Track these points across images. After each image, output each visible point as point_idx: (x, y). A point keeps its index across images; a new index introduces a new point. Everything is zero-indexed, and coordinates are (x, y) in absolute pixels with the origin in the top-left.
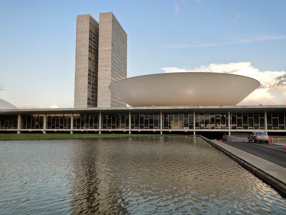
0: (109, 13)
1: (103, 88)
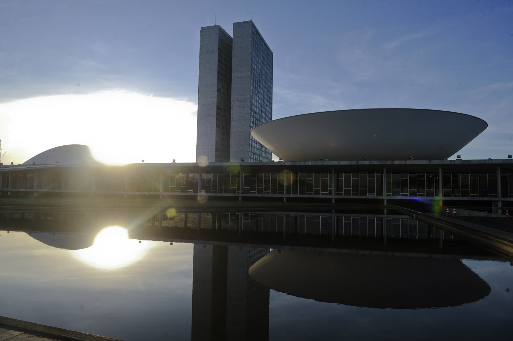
0: (247, 22)
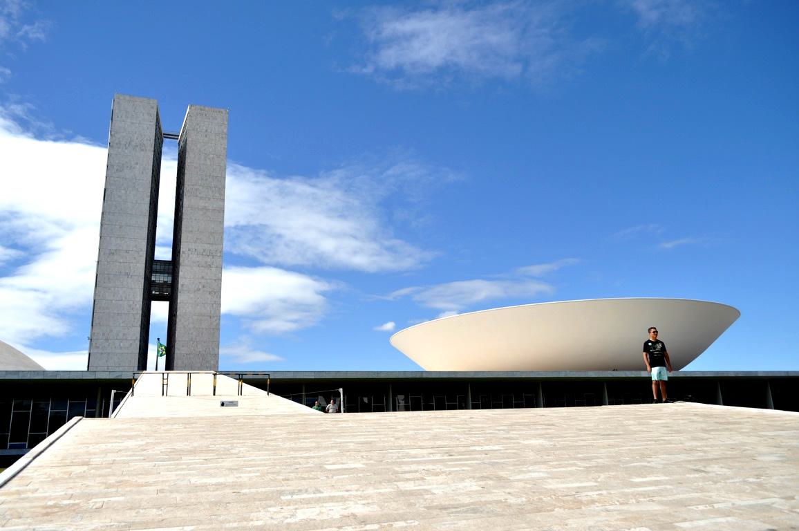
1: (195, 317)
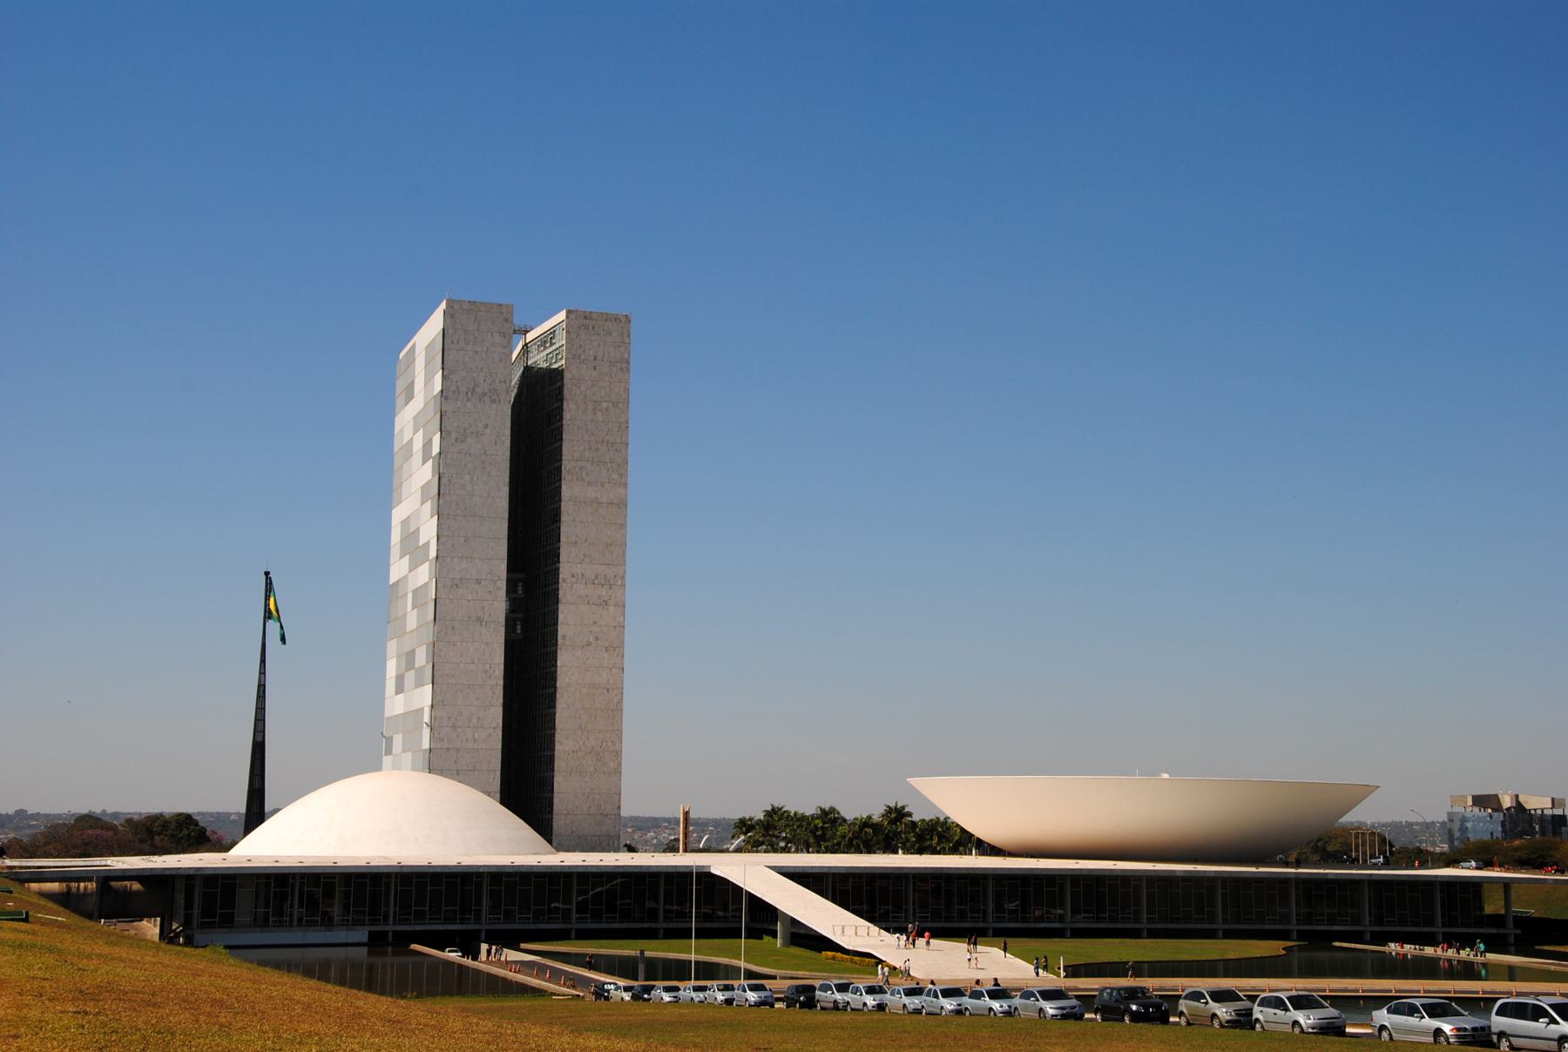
1: (584, 691)
